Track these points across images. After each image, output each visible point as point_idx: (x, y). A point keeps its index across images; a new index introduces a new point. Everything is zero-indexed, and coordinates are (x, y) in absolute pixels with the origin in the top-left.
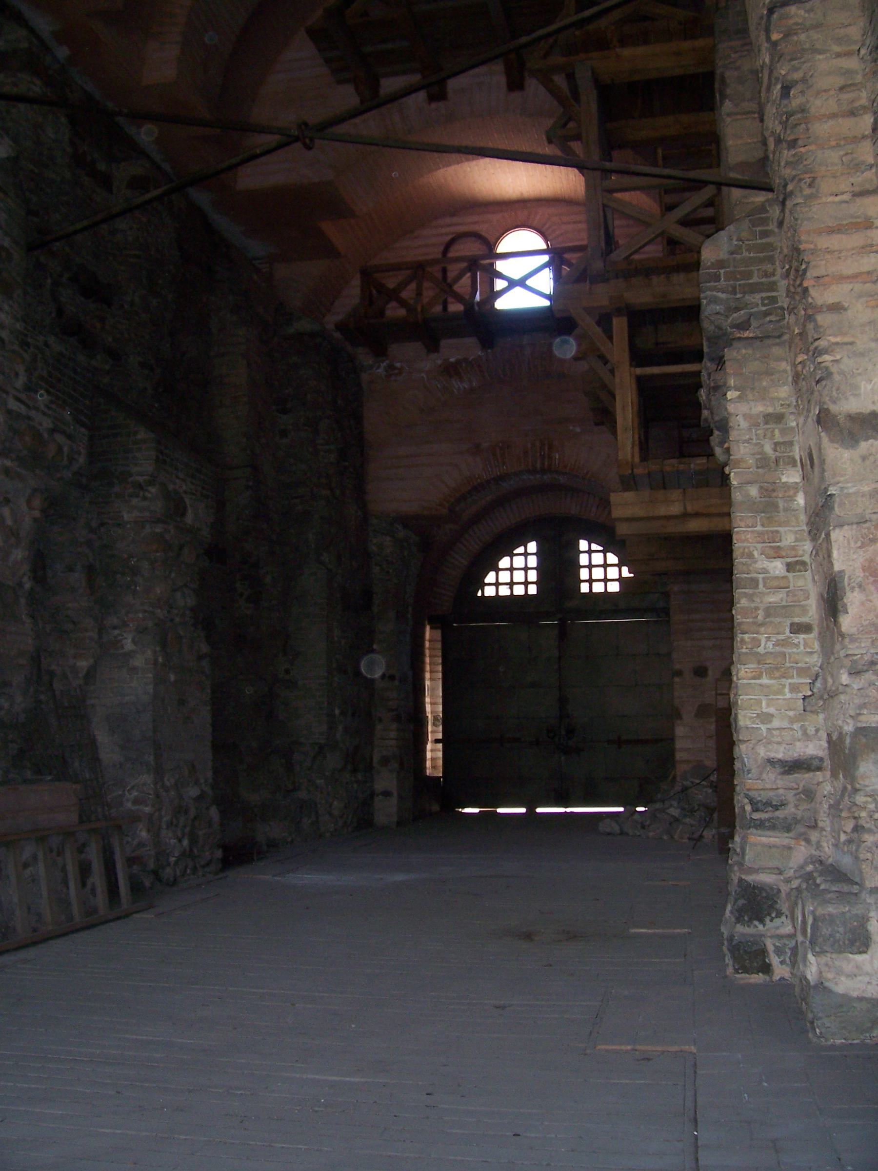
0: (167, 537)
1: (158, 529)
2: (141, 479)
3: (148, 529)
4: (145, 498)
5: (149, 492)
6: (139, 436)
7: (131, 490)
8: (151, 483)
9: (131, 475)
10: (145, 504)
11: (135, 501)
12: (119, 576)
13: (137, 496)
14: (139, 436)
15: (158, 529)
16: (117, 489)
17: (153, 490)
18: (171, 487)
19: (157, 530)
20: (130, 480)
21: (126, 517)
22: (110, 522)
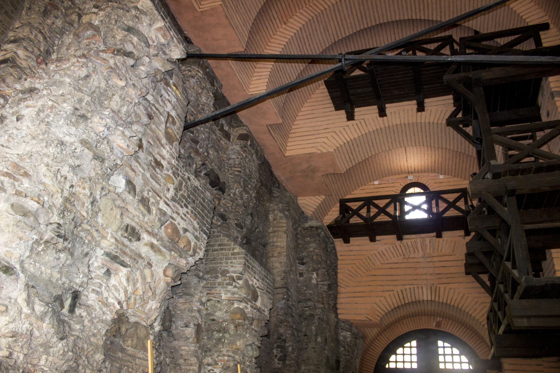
0: (246, 311)
1: (242, 306)
2: (235, 275)
3: (236, 305)
4: (235, 287)
5: (238, 283)
6: (235, 251)
7: (228, 281)
8: (239, 278)
9: (229, 273)
10: (236, 290)
11: (230, 287)
12: (215, 332)
13: (232, 285)
14: (235, 251)
15: (242, 306)
16: (219, 280)
17: (241, 282)
18: (250, 283)
19: (241, 307)
20: (228, 275)
21: (224, 297)
22: (214, 299)
